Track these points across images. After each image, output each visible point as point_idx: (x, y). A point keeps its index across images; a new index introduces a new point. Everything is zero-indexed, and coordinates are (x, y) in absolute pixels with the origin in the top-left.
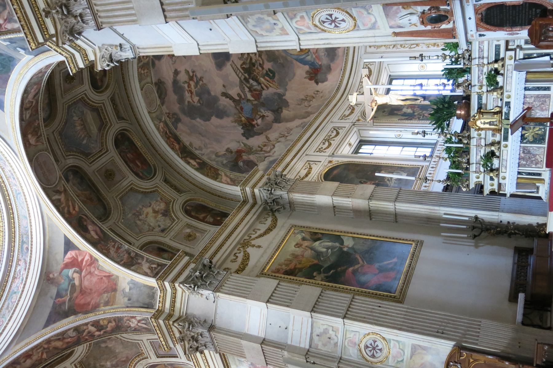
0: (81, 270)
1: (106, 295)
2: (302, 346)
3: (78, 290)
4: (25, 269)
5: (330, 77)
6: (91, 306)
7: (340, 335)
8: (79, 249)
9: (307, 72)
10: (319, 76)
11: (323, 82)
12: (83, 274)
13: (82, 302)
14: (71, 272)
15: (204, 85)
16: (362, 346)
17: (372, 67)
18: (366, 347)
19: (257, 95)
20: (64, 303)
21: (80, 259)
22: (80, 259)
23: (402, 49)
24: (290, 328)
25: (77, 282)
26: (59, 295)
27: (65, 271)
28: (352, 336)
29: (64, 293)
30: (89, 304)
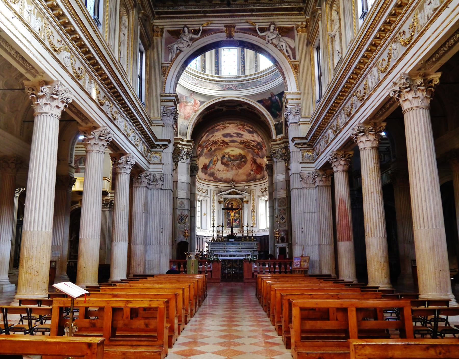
0: (192, 106)
1: (183, 115)
2: (178, 195)
3: (186, 104)
4: (195, 84)
5: (203, 174)
6: (180, 109)
7: (183, 208)
8: (200, 106)
9: (206, 164)
10: (204, 169)
11: (202, 171)
12: (191, 107)
13: (182, 106)
14: (193, 102)
15: (220, 130)
16: (182, 216)
17: (206, 193)
18: (181, 217)
19: (206, 147)
20: (183, 99)
21: (196, 106)
22: (196, 106)
23: (212, 206)
24: (182, 191)
25: (189, 104)
26: (186, 97)
27: (193, 100)
28: (184, 212)
29: (186, 99)
30: (181, 108)
